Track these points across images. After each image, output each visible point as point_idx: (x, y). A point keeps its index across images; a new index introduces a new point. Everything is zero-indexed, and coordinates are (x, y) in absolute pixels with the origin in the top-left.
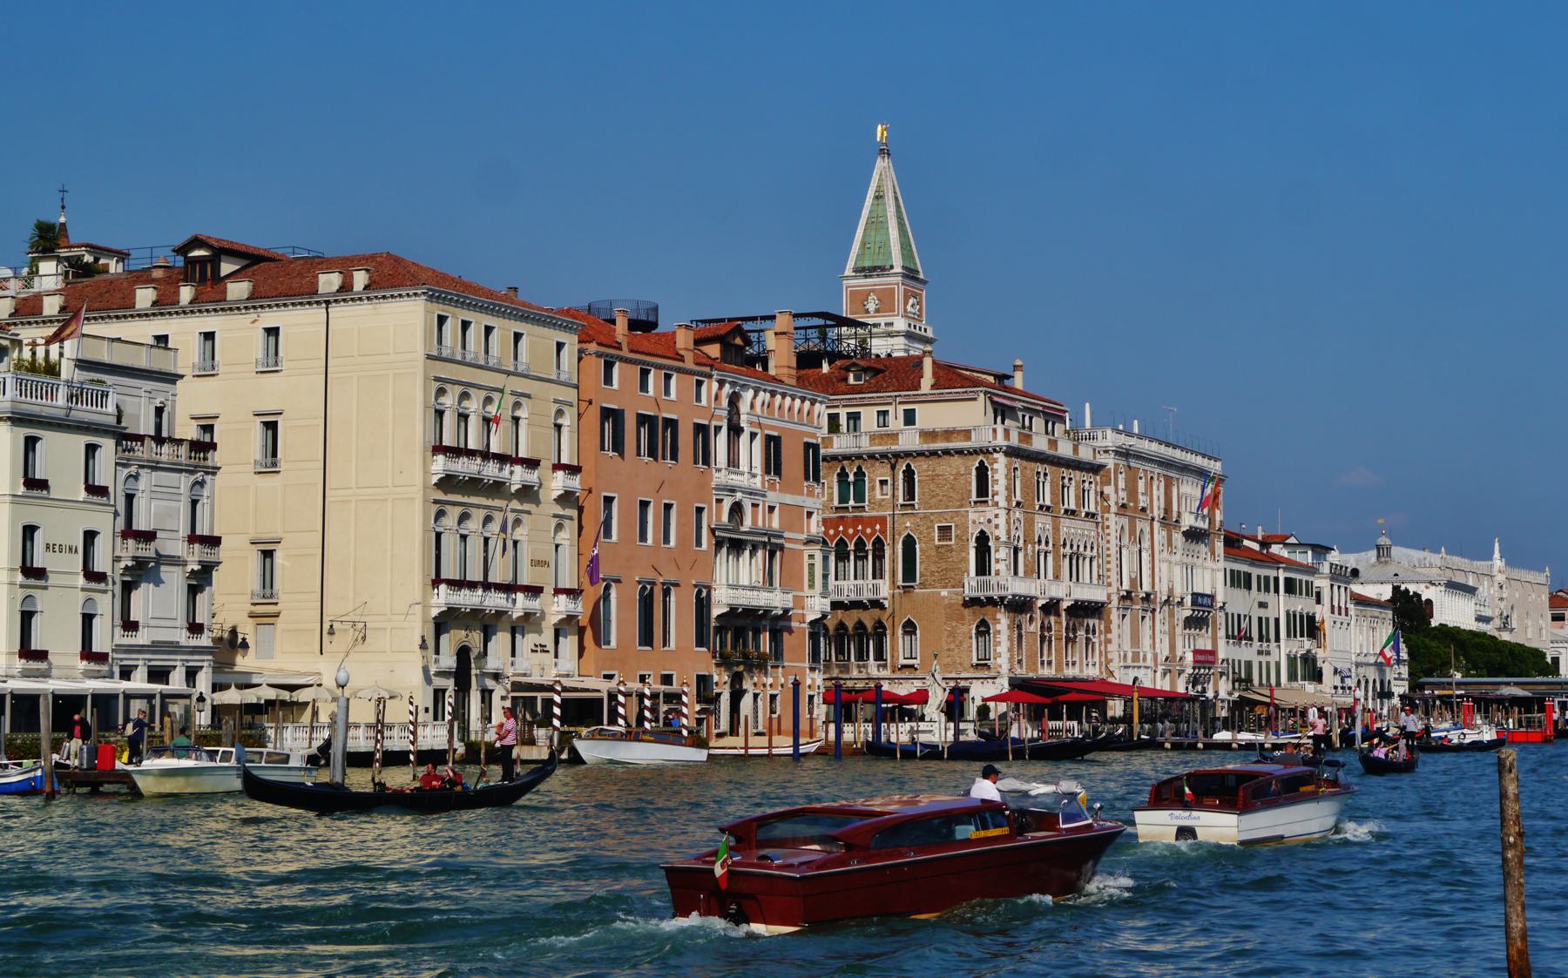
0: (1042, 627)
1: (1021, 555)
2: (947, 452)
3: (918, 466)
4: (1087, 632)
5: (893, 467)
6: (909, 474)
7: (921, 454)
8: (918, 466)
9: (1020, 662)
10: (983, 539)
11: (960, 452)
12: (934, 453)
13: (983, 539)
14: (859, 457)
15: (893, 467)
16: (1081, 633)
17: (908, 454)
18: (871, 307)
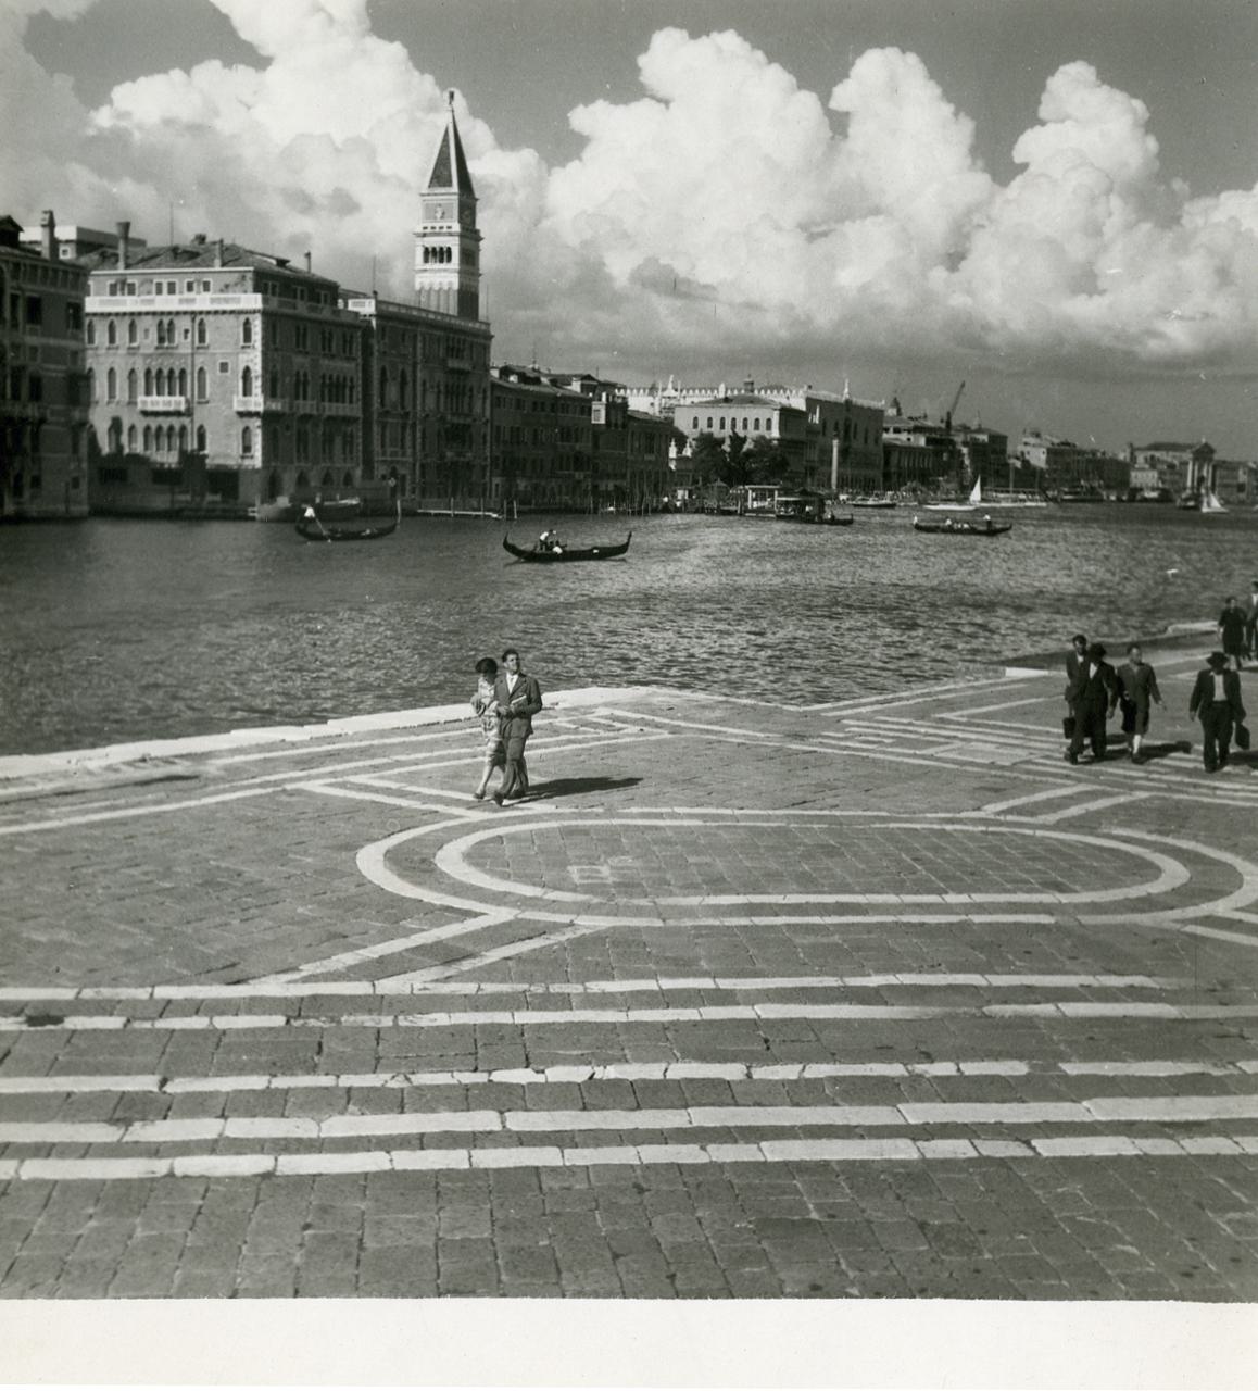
0: (299, 432)
1: (279, 386)
2: (224, 312)
3: (209, 320)
4: (345, 437)
5: (193, 320)
6: (201, 323)
7: (208, 313)
8: (209, 320)
9: (276, 456)
10: (247, 371)
11: (232, 312)
12: (216, 312)
13: (247, 371)
14: (170, 313)
15: (193, 320)
16: (338, 441)
17: (201, 313)
18: (439, 215)
